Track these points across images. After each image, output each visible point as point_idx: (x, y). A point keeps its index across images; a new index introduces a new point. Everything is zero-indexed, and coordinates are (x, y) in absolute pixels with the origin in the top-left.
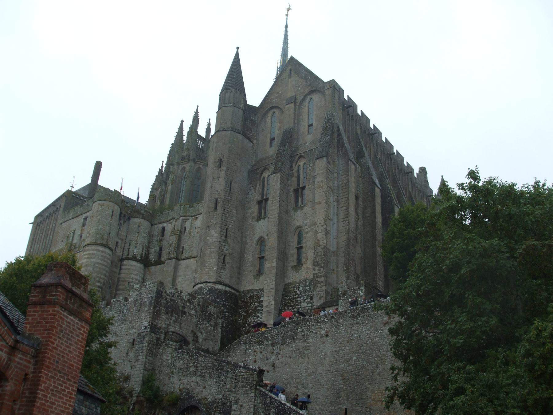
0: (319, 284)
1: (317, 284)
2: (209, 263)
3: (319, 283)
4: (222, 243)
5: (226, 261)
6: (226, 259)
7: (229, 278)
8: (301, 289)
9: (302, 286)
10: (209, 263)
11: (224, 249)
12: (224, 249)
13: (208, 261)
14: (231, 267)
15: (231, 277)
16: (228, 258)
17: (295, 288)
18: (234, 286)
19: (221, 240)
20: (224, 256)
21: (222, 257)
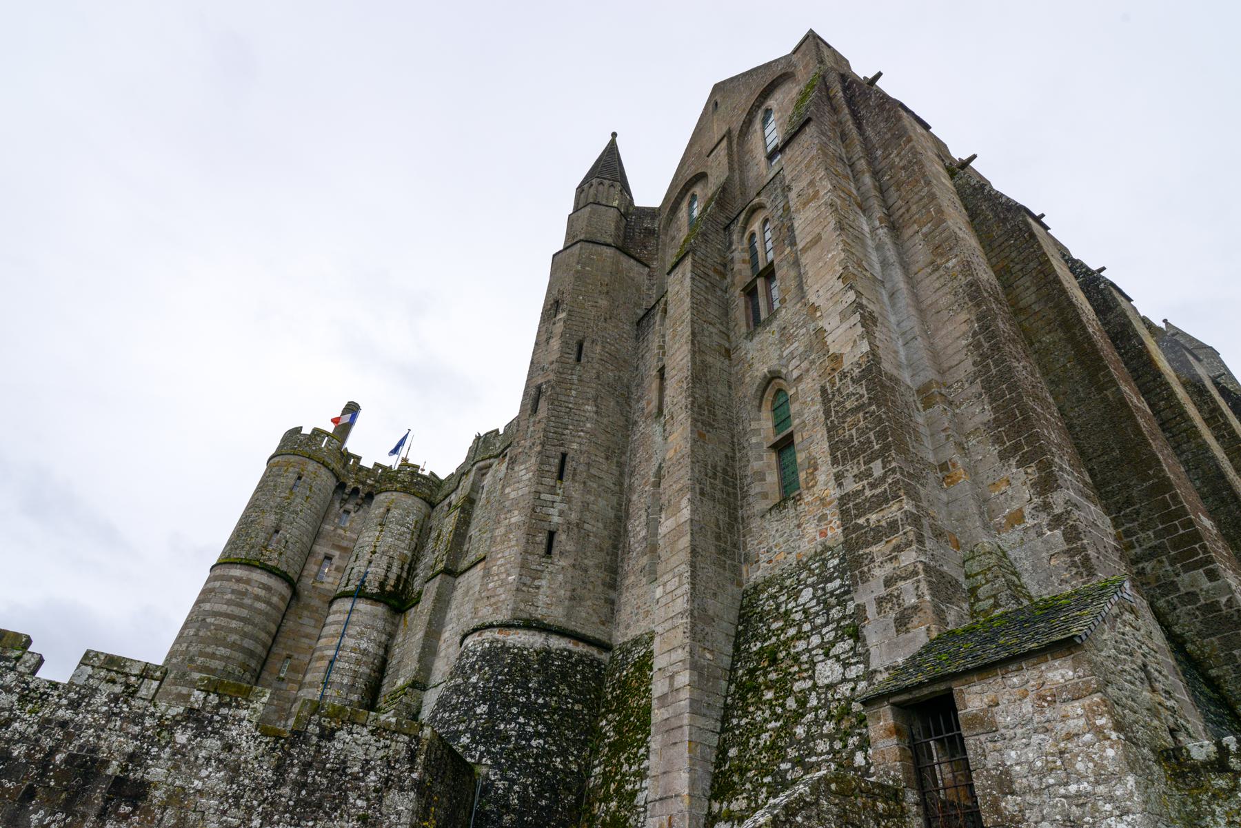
0: (877, 540)
1: (868, 544)
2: (499, 563)
3: (878, 534)
4: (543, 496)
5: (555, 551)
6: (555, 544)
7: (567, 603)
8: (807, 594)
9: (810, 581)
10: (499, 563)
11: (551, 511)
12: (551, 511)
13: (499, 556)
14: (574, 566)
15: (572, 598)
16: (563, 537)
17: (783, 598)
18: (589, 631)
19: (541, 488)
20: (551, 535)
21: (542, 538)
